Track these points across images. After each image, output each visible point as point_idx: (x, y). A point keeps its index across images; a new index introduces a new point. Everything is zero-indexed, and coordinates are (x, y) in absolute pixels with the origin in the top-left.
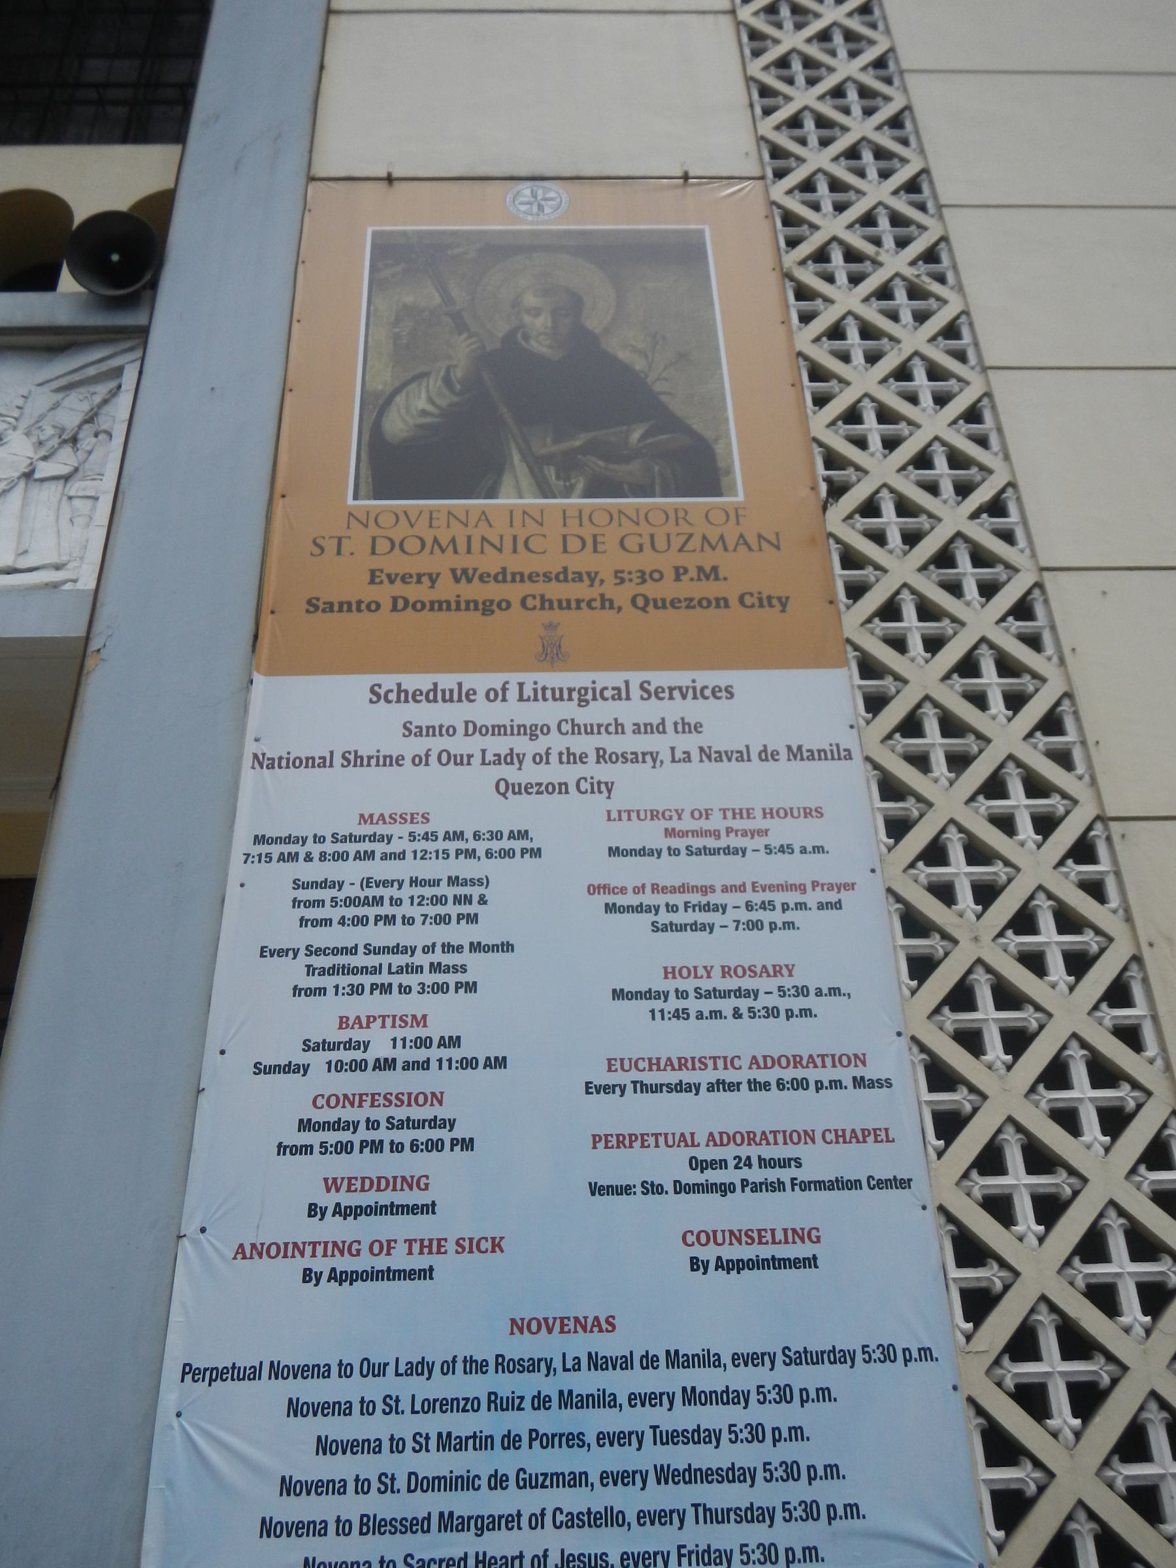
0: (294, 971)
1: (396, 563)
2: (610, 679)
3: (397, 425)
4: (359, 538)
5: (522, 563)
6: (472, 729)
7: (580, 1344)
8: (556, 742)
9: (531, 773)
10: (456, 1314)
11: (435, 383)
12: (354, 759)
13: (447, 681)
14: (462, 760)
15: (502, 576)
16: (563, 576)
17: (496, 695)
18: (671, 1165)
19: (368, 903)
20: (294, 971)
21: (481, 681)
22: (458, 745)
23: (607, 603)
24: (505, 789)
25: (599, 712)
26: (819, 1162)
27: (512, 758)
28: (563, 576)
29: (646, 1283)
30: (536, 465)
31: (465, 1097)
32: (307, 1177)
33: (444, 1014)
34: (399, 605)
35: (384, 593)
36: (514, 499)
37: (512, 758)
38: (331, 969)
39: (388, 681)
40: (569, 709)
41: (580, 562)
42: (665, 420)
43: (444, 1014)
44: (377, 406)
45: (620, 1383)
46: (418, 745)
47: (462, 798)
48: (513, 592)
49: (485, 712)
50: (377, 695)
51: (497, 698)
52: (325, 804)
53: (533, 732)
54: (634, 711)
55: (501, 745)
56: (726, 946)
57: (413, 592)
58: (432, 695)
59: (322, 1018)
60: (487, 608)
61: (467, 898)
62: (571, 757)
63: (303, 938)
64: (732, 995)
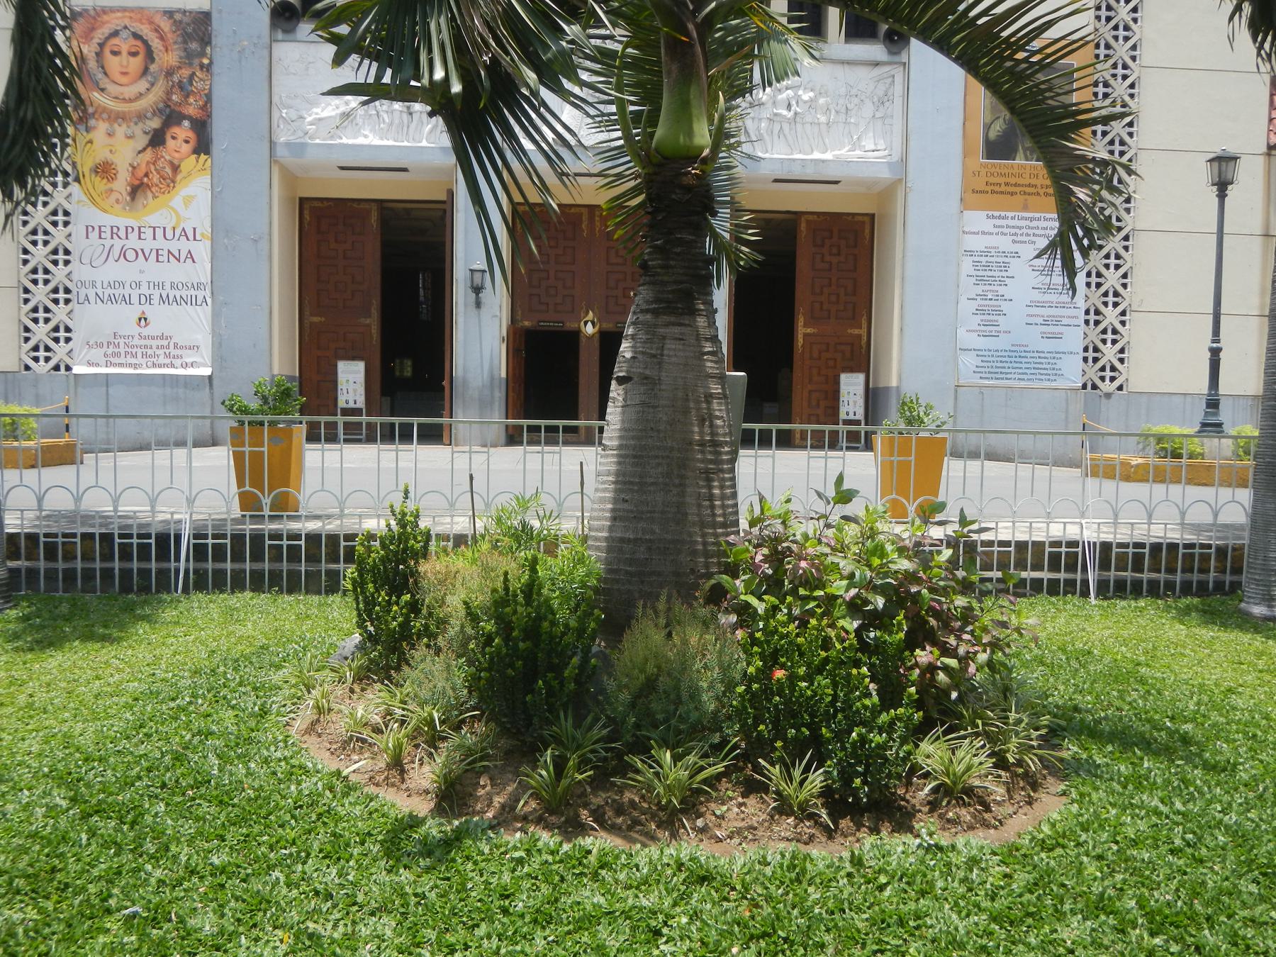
0: (973, 280)
1: (992, 180)
2: (1037, 215)
3: (993, 135)
4: (983, 173)
5: (1021, 181)
6: (1008, 227)
7: (1022, 349)
8: (1025, 231)
9: (1020, 238)
10: (1002, 343)
11: (1001, 120)
12: (983, 233)
13: (1003, 214)
14: (1003, 234)
15: (1016, 185)
16: (1029, 185)
17: (1013, 218)
18: (1040, 320)
19: (987, 266)
20: (973, 280)
21: (1010, 214)
22: (1005, 230)
23: (1038, 194)
24: (1014, 242)
25: (1035, 224)
26: (1065, 321)
27: (1016, 234)
28: (1029, 185)
29: (1034, 339)
30: (1025, 150)
31: (1005, 306)
32: (978, 319)
33: (1002, 290)
34: (993, 192)
35: (989, 188)
36: (1019, 161)
37: (1016, 234)
38: (980, 280)
39: (990, 213)
40: (1028, 223)
41: (1033, 182)
43: (1002, 290)
44: (987, 127)
45: (1028, 355)
46: (997, 230)
47: (1004, 243)
48: (1018, 189)
49: (1011, 223)
50: (988, 217)
53: (1020, 228)
55: (1013, 231)
57: (997, 188)
58: (999, 217)
59: (979, 290)
60: (1012, 194)
61: (1006, 266)
62: (1028, 235)
63: (975, 273)
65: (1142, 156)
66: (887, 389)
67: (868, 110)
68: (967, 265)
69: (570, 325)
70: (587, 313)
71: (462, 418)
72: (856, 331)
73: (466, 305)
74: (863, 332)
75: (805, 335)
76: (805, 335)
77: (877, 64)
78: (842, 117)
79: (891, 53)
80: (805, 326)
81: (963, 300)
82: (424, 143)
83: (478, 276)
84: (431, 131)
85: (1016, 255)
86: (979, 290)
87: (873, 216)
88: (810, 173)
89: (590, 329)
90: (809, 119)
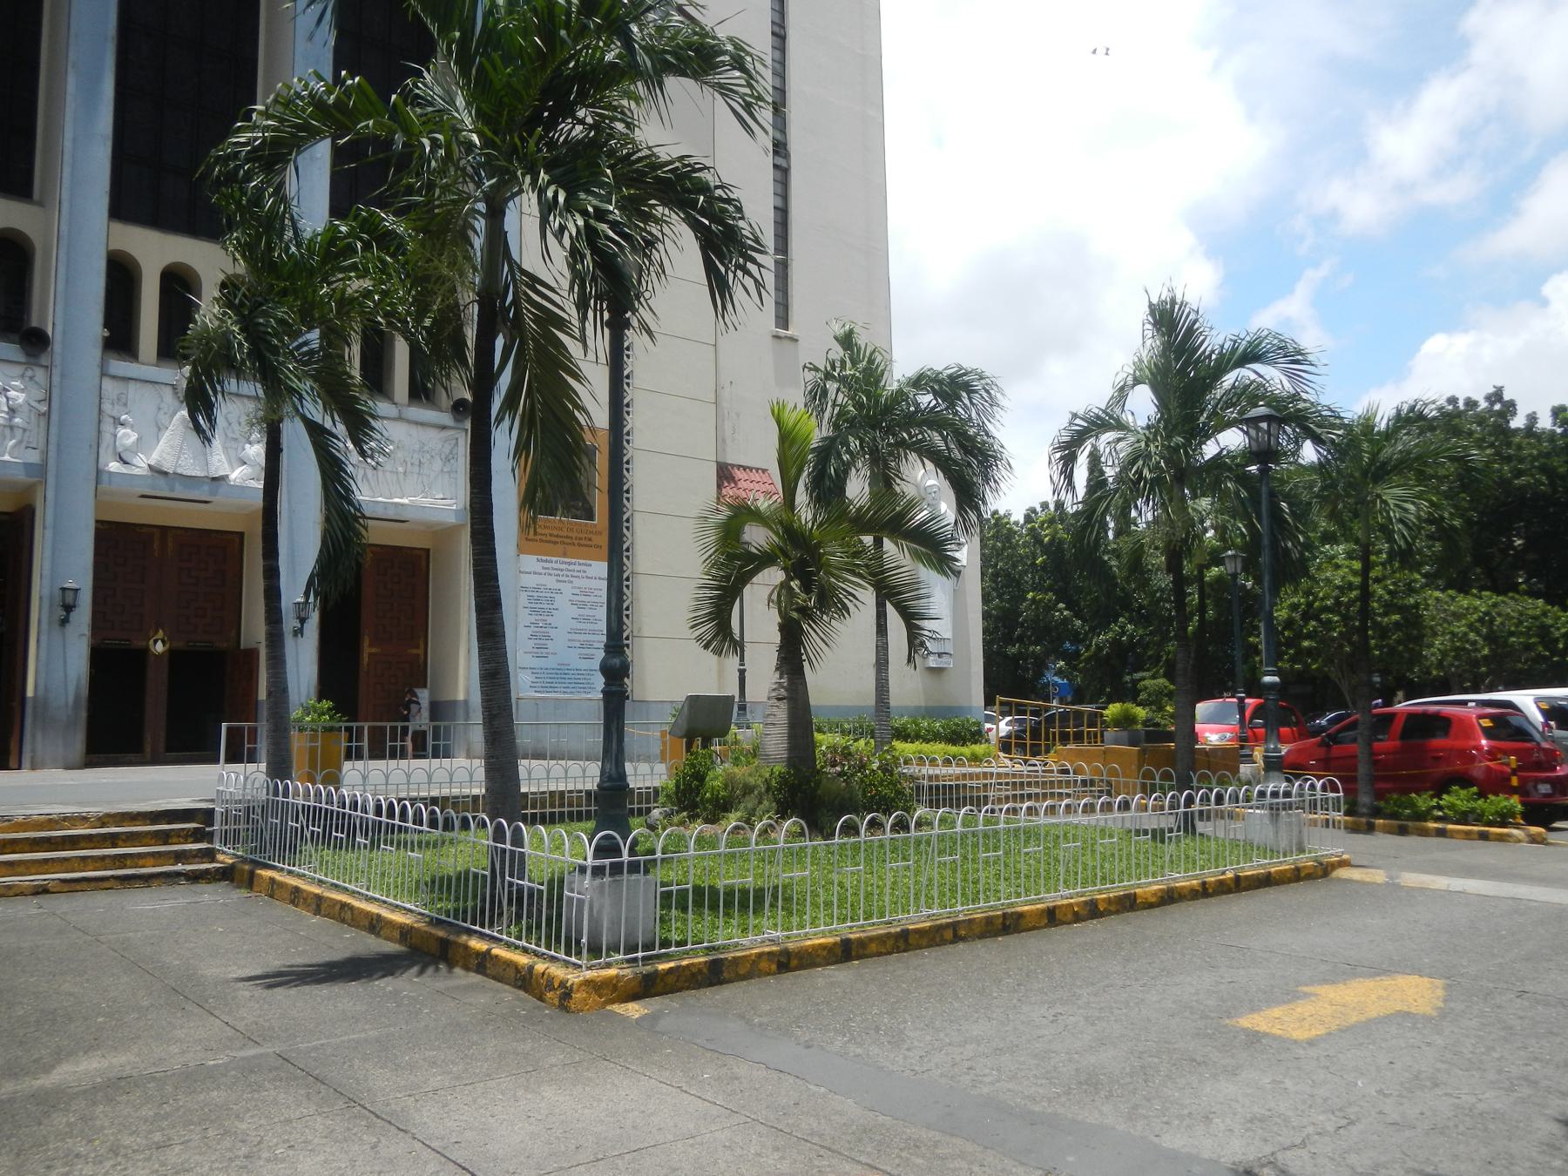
10: (551, 663)
31: (552, 632)
32: (532, 643)
33: (549, 619)
38: (534, 610)
42: (585, 501)
43: (549, 619)
47: (550, 582)
51: (557, 562)
52: (530, 581)
54: (577, 568)
56: (587, 612)
59: (533, 618)
64: (587, 619)
65: (637, 517)
66: (454, 703)
67: (438, 464)
68: (523, 597)
69: (138, 643)
70: (156, 632)
71: (34, 739)
72: (414, 651)
73: (50, 623)
74: (421, 651)
75: (370, 654)
76: (370, 654)
77: (444, 428)
78: (416, 469)
79: (456, 420)
80: (371, 645)
81: (521, 626)
82: (7, 458)
83: (70, 595)
84: (15, 446)
85: (559, 592)
86: (533, 618)
87: (427, 551)
88: (391, 514)
89: (160, 647)
90: (388, 467)
